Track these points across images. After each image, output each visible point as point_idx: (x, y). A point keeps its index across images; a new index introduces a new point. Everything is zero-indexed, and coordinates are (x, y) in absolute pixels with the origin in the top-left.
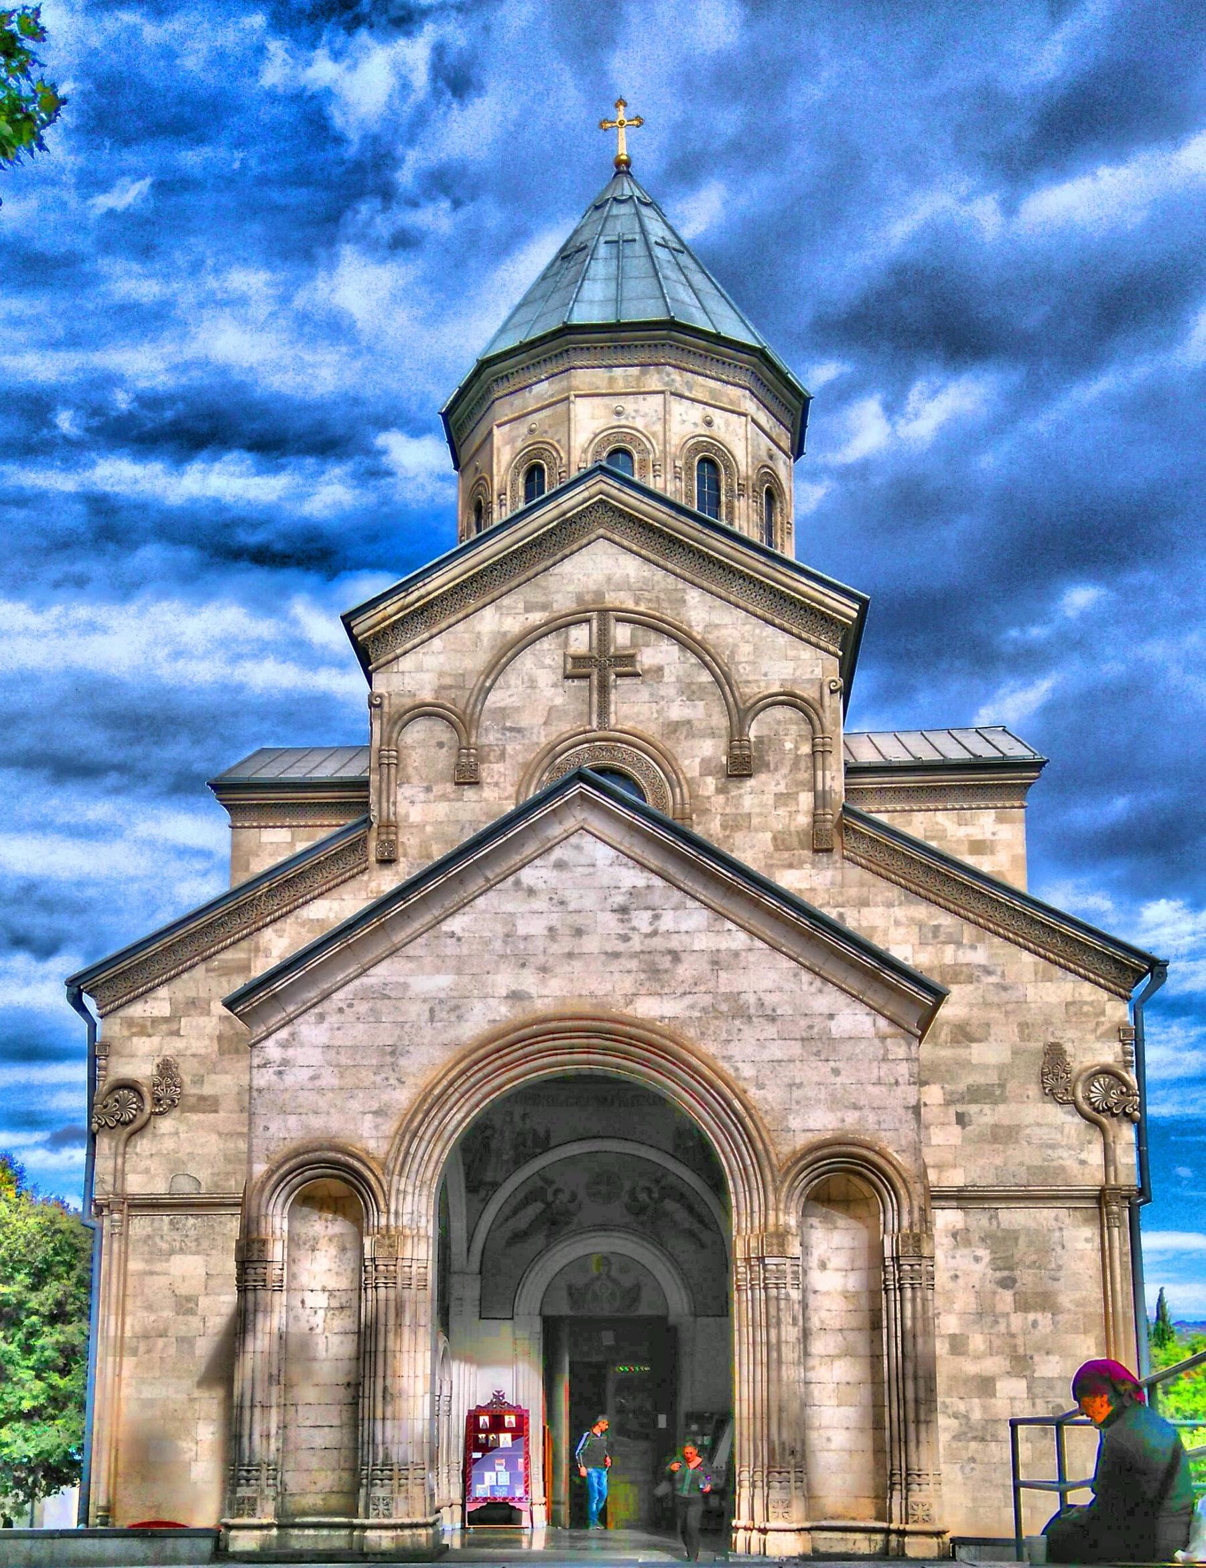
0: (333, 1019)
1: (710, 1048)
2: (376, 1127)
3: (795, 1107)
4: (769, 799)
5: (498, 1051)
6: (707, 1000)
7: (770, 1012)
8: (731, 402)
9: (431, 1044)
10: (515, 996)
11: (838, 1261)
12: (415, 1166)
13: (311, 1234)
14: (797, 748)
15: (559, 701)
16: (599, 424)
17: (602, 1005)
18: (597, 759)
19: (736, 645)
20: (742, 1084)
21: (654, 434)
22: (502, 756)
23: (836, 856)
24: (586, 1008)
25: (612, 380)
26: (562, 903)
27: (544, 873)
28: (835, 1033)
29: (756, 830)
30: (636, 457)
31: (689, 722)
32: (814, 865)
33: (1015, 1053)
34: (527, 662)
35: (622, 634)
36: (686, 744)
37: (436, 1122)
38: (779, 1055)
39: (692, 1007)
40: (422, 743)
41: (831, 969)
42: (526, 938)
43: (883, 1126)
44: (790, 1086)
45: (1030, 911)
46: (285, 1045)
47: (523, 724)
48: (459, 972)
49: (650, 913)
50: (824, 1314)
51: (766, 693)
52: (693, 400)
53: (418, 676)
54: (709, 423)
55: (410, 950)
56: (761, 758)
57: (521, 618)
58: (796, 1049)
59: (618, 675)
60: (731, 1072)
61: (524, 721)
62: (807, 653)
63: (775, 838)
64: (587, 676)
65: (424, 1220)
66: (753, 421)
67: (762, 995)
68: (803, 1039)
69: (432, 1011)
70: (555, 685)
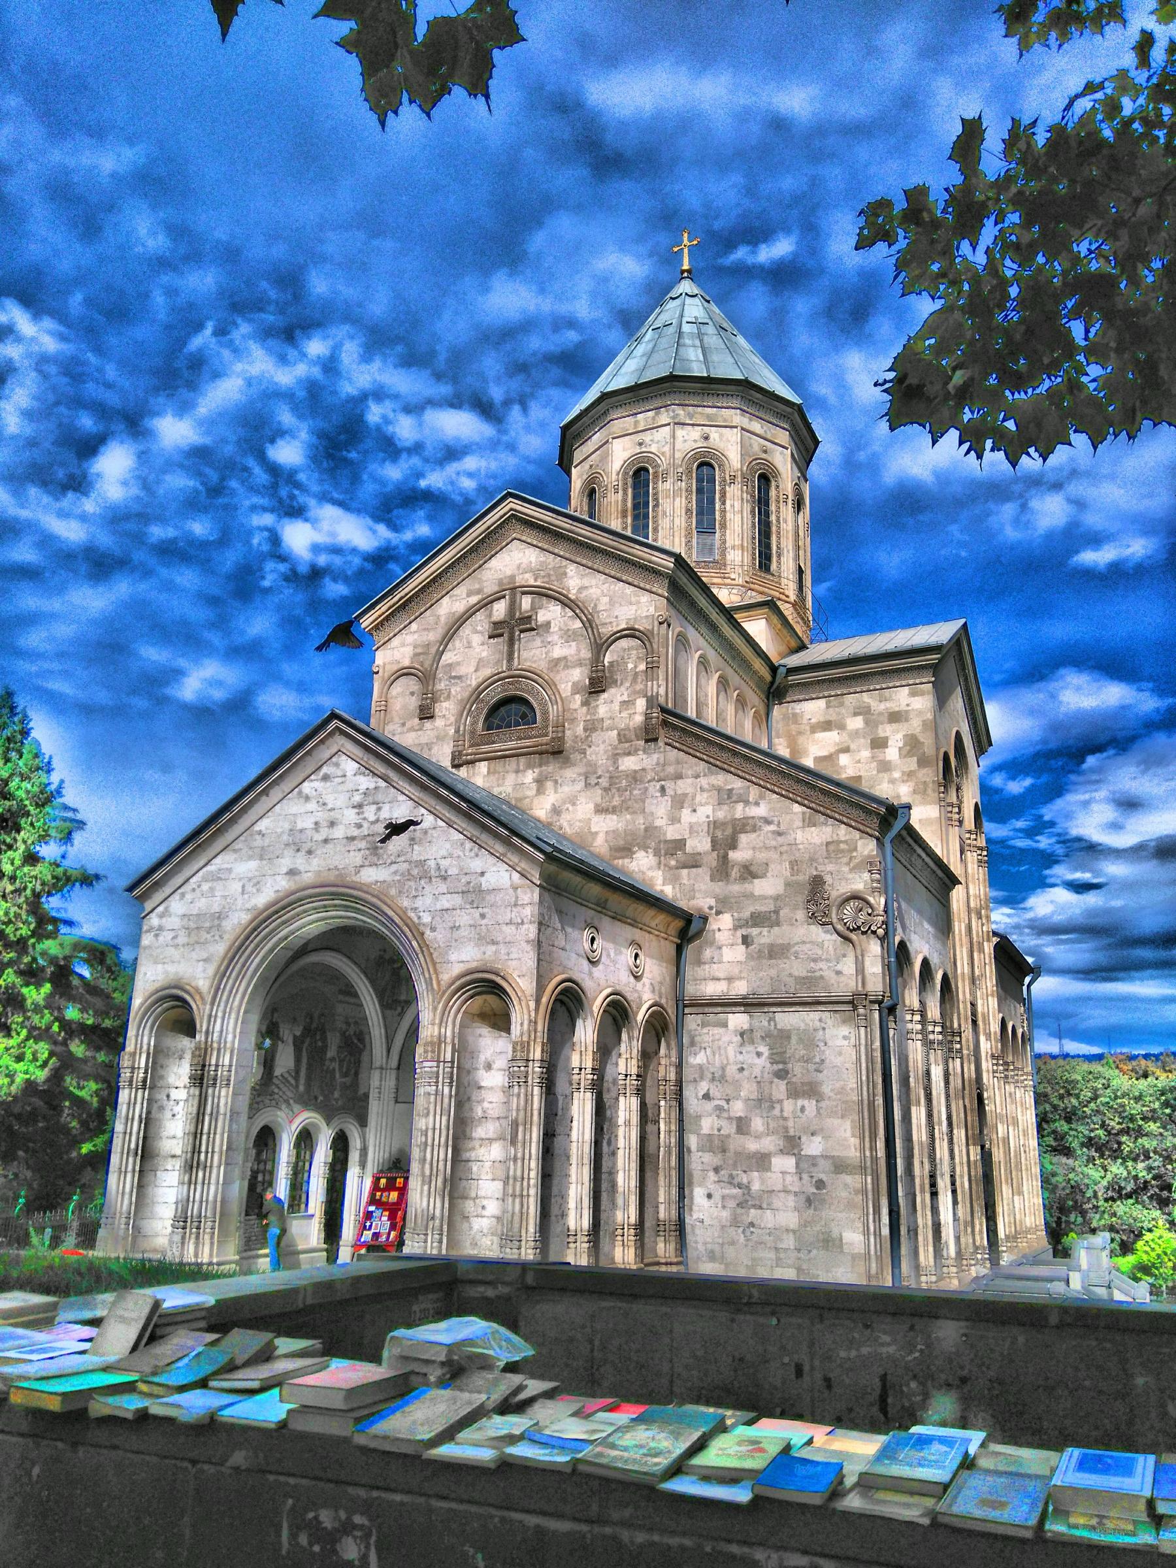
0: (189, 897)
1: (405, 903)
2: (204, 971)
3: (453, 944)
4: (616, 706)
5: (277, 912)
6: (406, 866)
7: (443, 873)
8: (725, 420)
9: (241, 910)
10: (292, 872)
11: (501, 1063)
12: (224, 998)
13: (180, 1046)
14: (636, 667)
15: (484, 654)
16: (627, 455)
17: (341, 875)
18: (505, 691)
19: (598, 599)
20: (422, 928)
21: (663, 454)
22: (448, 697)
23: (661, 743)
24: (332, 877)
25: (636, 423)
26: (324, 804)
27: (316, 784)
28: (484, 887)
29: (607, 730)
30: (651, 471)
31: (565, 658)
32: (644, 751)
33: (787, 885)
34: (466, 630)
35: (526, 602)
36: (563, 674)
37: (239, 965)
38: (447, 905)
39: (395, 873)
40: (402, 694)
41: (485, 837)
42: (301, 831)
43: (512, 956)
44: (452, 928)
45: (793, 772)
46: (161, 916)
47: (461, 673)
48: (261, 859)
49: (374, 807)
50: (486, 1105)
51: (615, 630)
52: (693, 425)
53: (402, 649)
54: (706, 438)
55: (236, 846)
56: (611, 677)
57: (464, 602)
58: (457, 900)
59: (522, 631)
60: (416, 920)
61: (462, 670)
62: (645, 598)
63: (619, 734)
64: (501, 635)
65: (230, 1038)
66: (743, 429)
67: (439, 861)
68: (463, 892)
69: (243, 886)
70: (483, 644)
